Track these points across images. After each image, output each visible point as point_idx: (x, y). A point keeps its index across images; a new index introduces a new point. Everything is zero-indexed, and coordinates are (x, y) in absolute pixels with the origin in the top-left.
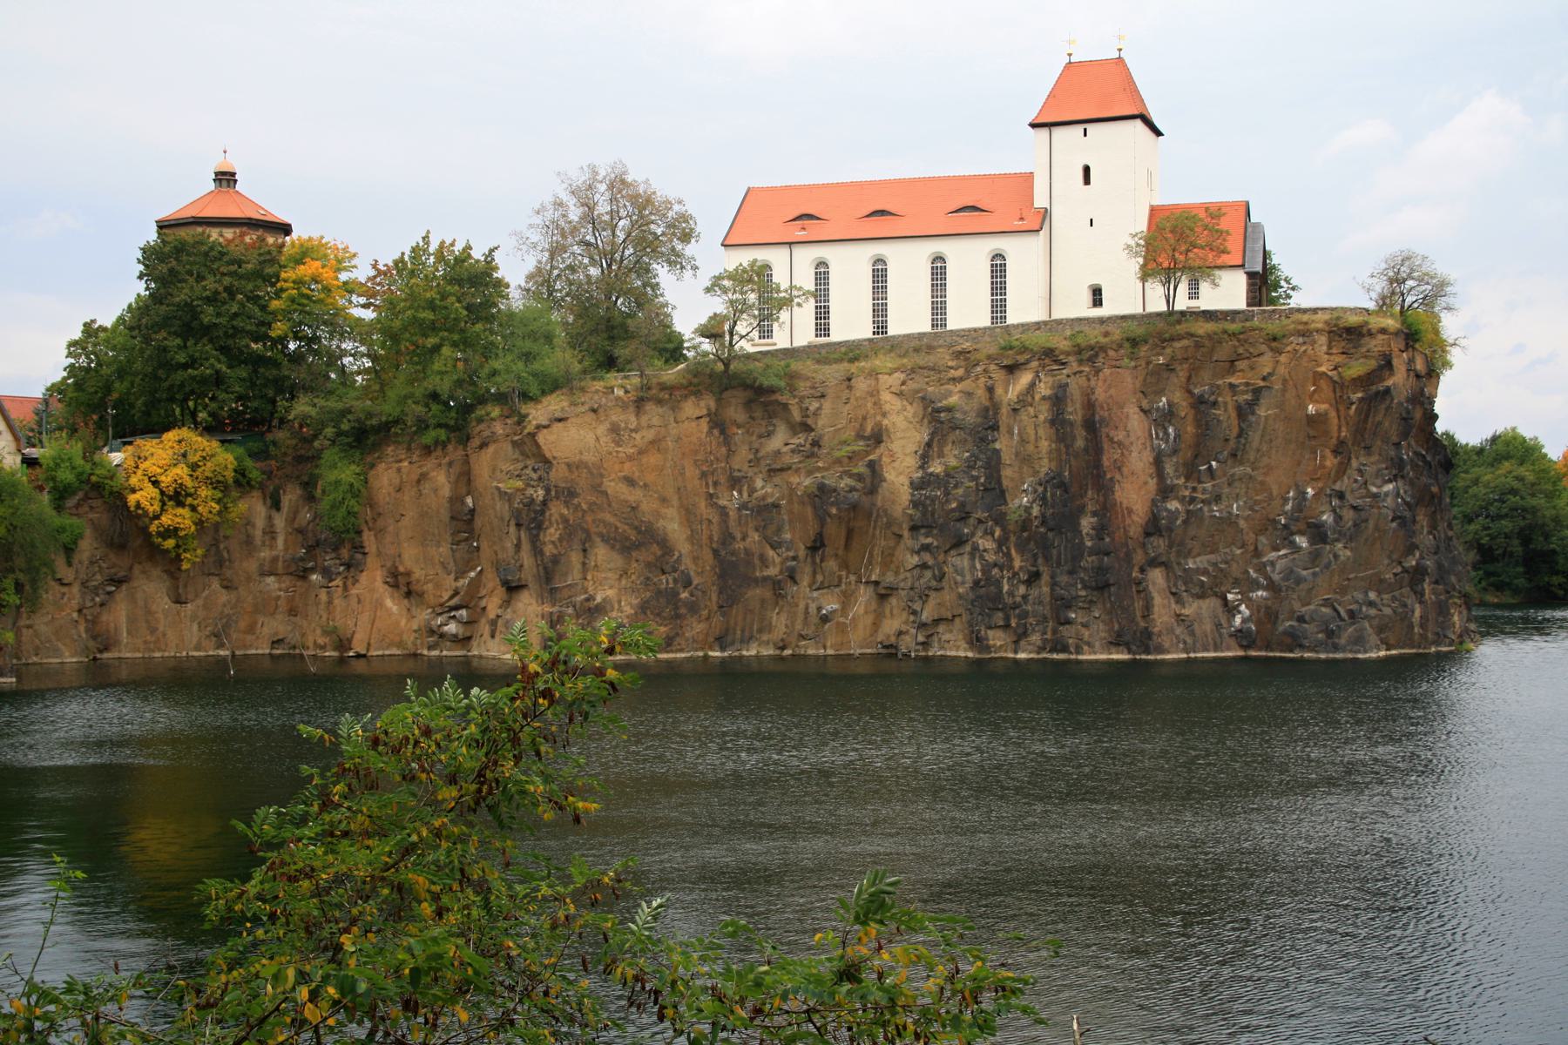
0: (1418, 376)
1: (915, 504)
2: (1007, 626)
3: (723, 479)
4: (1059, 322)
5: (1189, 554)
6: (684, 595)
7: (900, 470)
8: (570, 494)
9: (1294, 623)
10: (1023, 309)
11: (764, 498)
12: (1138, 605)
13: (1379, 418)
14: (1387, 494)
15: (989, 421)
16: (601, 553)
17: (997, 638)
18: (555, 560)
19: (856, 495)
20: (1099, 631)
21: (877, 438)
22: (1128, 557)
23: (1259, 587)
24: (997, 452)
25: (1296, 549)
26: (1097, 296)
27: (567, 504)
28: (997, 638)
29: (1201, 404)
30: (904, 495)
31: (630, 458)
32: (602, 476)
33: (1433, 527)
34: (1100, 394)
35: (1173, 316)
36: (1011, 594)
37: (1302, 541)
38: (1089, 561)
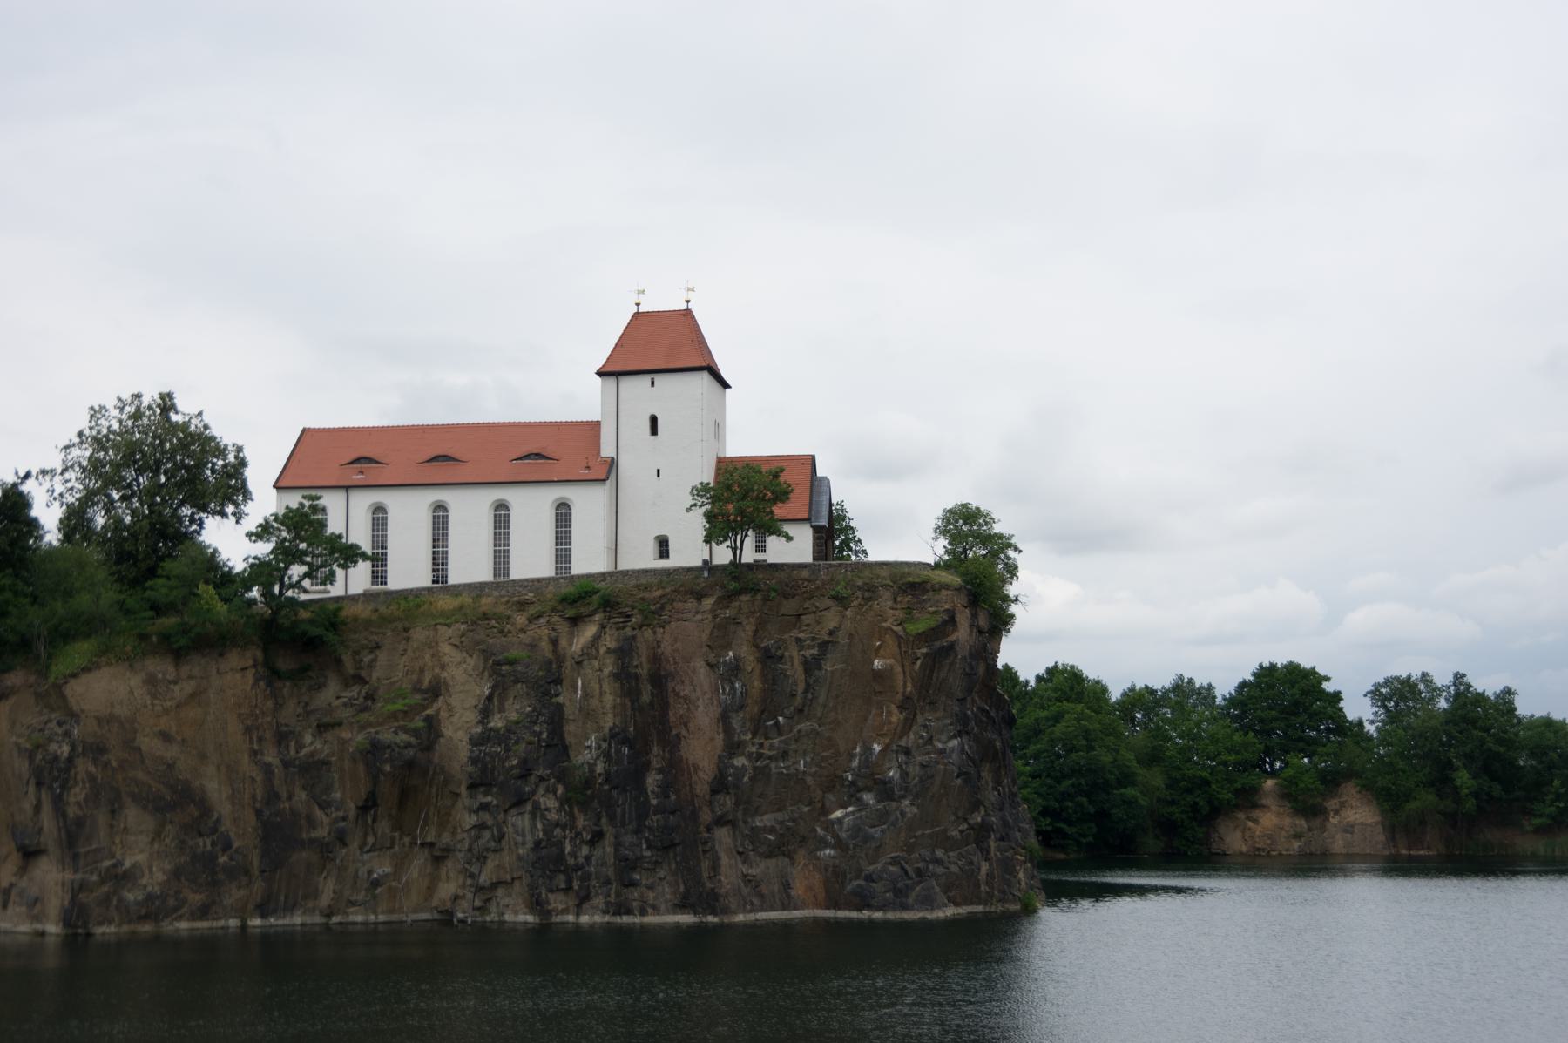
0: (980, 632)
1: (474, 761)
2: (568, 889)
3: (268, 735)
4: (625, 573)
5: (758, 812)
6: (223, 859)
7: (459, 725)
8: (97, 750)
9: (862, 883)
10: (589, 560)
11: (312, 754)
12: (706, 864)
13: (942, 675)
14: (952, 749)
15: (550, 678)
16: (132, 814)
17: (556, 901)
18: (80, 822)
19: (411, 752)
20: (667, 892)
21: (436, 691)
22: (694, 815)
23: (827, 845)
24: (560, 707)
25: (863, 806)
26: (663, 547)
27: (95, 761)
28: (556, 901)
29: (769, 658)
30: (464, 751)
31: (166, 712)
32: (135, 732)
33: (998, 782)
34: (666, 648)
35: (736, 569)
36: (573, 854)
37: (869, 798)
38: (655, 820)
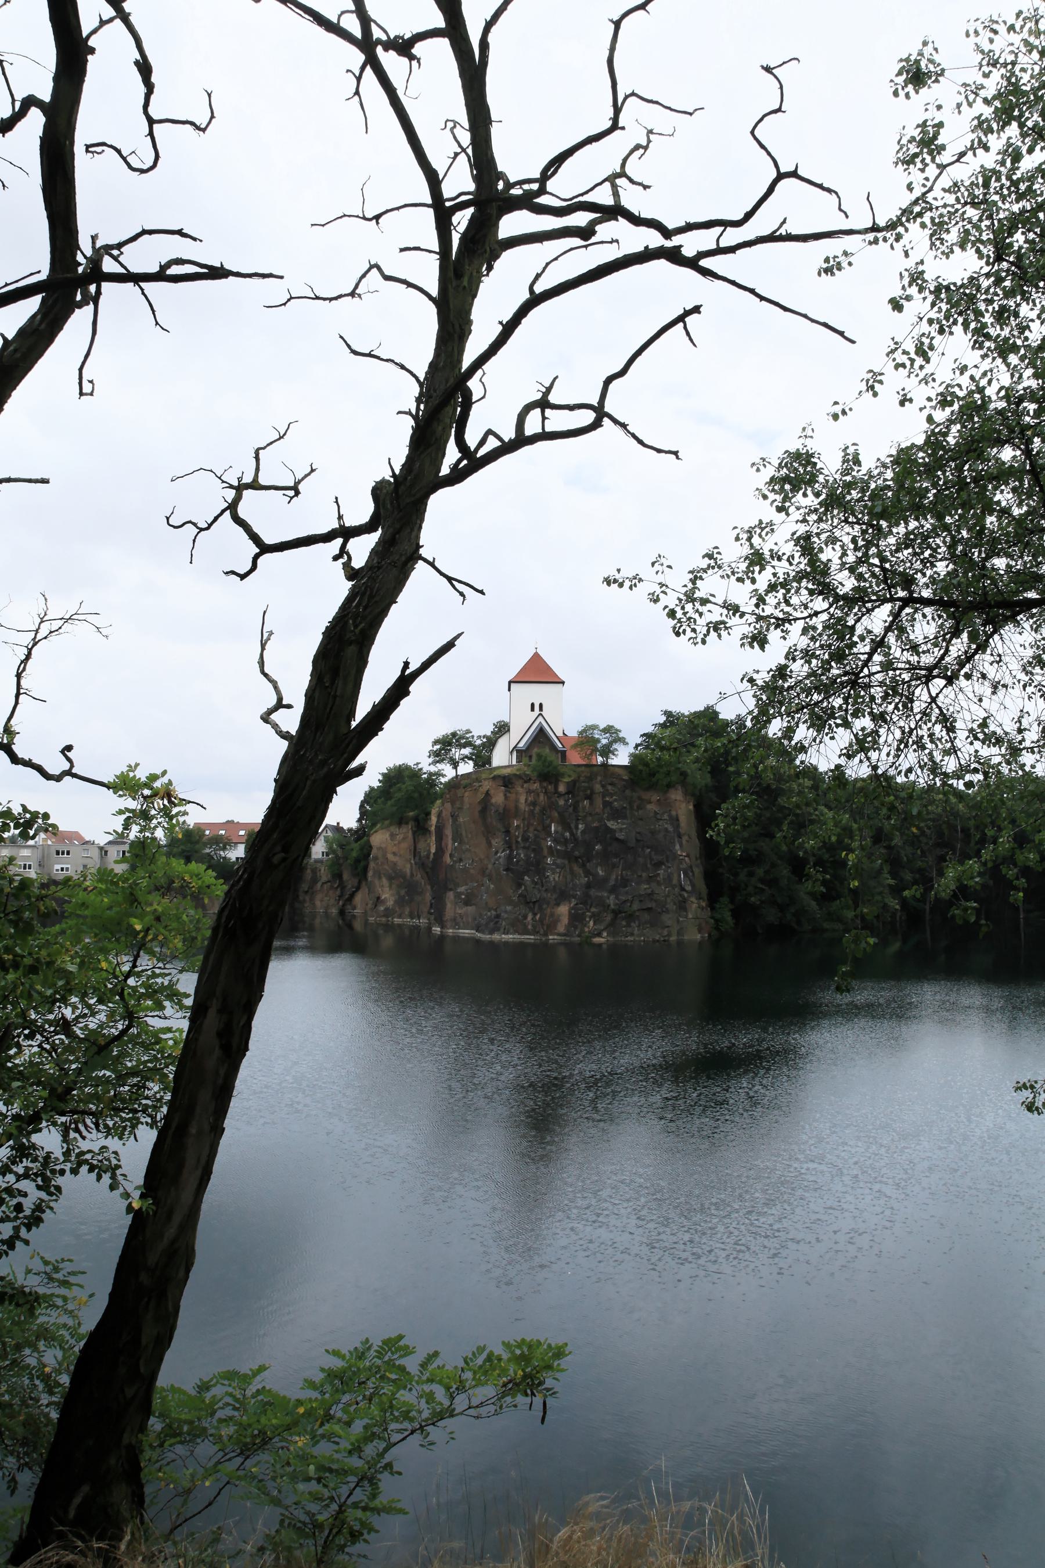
16: (384, 880)
